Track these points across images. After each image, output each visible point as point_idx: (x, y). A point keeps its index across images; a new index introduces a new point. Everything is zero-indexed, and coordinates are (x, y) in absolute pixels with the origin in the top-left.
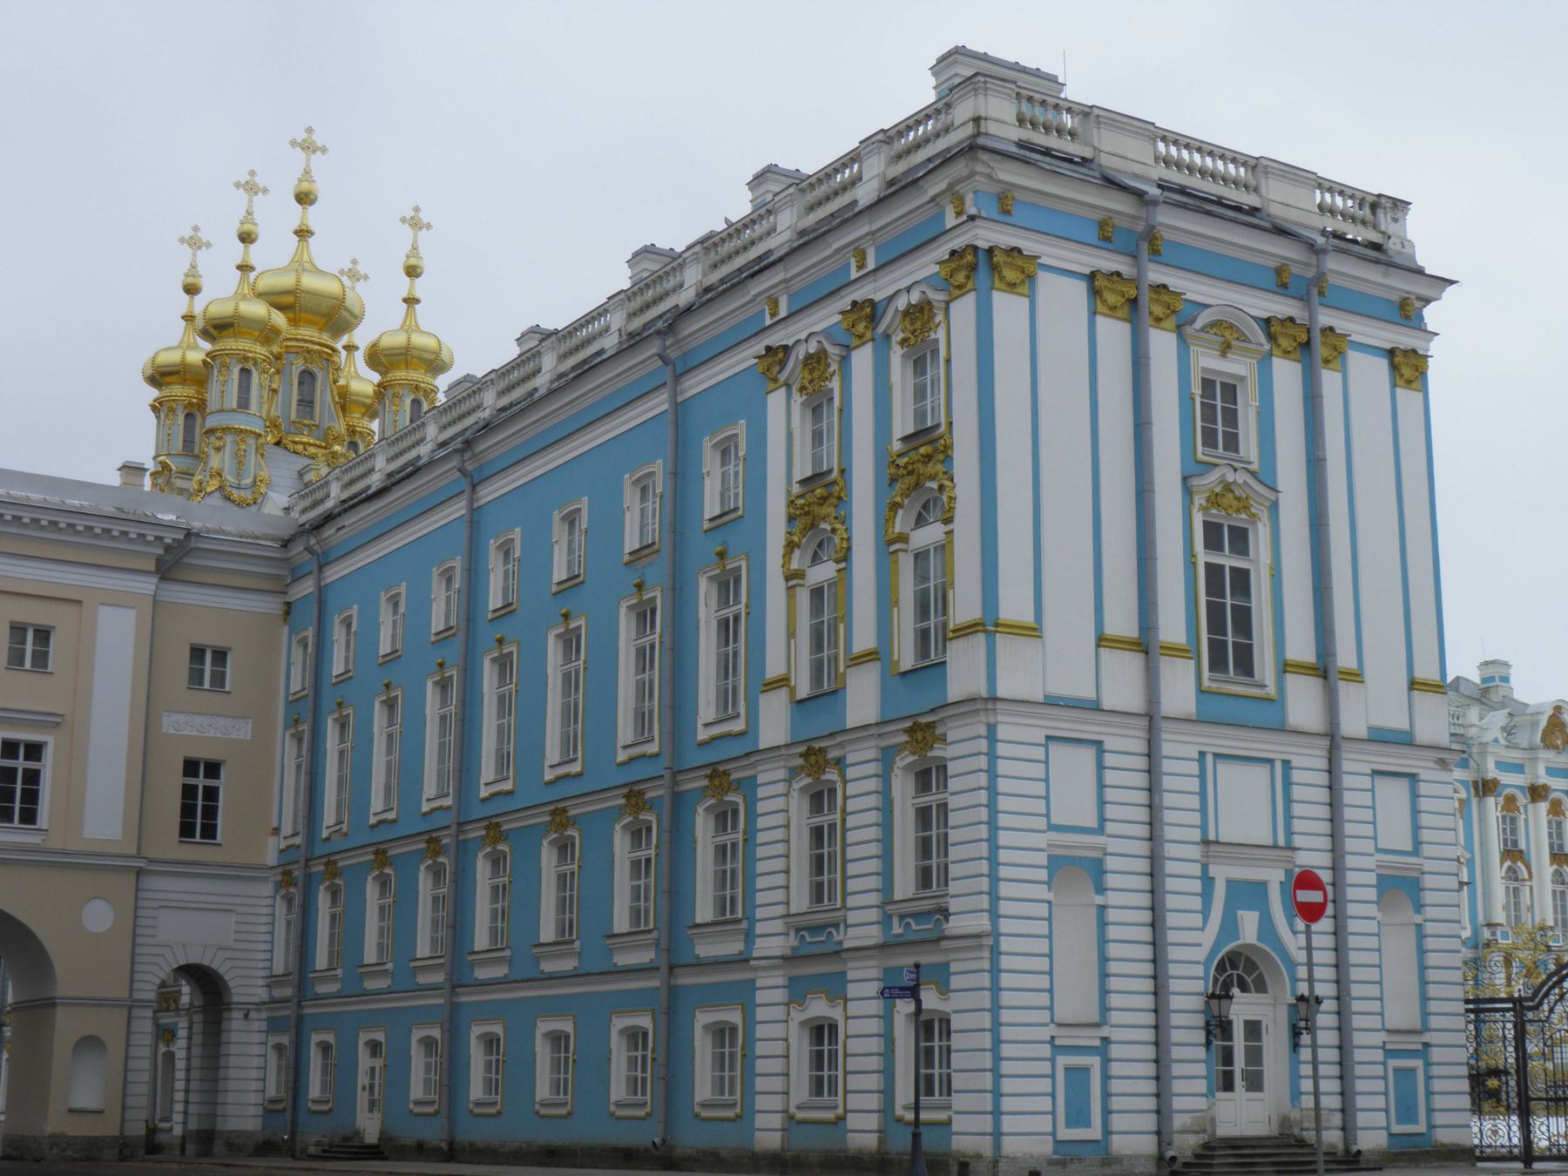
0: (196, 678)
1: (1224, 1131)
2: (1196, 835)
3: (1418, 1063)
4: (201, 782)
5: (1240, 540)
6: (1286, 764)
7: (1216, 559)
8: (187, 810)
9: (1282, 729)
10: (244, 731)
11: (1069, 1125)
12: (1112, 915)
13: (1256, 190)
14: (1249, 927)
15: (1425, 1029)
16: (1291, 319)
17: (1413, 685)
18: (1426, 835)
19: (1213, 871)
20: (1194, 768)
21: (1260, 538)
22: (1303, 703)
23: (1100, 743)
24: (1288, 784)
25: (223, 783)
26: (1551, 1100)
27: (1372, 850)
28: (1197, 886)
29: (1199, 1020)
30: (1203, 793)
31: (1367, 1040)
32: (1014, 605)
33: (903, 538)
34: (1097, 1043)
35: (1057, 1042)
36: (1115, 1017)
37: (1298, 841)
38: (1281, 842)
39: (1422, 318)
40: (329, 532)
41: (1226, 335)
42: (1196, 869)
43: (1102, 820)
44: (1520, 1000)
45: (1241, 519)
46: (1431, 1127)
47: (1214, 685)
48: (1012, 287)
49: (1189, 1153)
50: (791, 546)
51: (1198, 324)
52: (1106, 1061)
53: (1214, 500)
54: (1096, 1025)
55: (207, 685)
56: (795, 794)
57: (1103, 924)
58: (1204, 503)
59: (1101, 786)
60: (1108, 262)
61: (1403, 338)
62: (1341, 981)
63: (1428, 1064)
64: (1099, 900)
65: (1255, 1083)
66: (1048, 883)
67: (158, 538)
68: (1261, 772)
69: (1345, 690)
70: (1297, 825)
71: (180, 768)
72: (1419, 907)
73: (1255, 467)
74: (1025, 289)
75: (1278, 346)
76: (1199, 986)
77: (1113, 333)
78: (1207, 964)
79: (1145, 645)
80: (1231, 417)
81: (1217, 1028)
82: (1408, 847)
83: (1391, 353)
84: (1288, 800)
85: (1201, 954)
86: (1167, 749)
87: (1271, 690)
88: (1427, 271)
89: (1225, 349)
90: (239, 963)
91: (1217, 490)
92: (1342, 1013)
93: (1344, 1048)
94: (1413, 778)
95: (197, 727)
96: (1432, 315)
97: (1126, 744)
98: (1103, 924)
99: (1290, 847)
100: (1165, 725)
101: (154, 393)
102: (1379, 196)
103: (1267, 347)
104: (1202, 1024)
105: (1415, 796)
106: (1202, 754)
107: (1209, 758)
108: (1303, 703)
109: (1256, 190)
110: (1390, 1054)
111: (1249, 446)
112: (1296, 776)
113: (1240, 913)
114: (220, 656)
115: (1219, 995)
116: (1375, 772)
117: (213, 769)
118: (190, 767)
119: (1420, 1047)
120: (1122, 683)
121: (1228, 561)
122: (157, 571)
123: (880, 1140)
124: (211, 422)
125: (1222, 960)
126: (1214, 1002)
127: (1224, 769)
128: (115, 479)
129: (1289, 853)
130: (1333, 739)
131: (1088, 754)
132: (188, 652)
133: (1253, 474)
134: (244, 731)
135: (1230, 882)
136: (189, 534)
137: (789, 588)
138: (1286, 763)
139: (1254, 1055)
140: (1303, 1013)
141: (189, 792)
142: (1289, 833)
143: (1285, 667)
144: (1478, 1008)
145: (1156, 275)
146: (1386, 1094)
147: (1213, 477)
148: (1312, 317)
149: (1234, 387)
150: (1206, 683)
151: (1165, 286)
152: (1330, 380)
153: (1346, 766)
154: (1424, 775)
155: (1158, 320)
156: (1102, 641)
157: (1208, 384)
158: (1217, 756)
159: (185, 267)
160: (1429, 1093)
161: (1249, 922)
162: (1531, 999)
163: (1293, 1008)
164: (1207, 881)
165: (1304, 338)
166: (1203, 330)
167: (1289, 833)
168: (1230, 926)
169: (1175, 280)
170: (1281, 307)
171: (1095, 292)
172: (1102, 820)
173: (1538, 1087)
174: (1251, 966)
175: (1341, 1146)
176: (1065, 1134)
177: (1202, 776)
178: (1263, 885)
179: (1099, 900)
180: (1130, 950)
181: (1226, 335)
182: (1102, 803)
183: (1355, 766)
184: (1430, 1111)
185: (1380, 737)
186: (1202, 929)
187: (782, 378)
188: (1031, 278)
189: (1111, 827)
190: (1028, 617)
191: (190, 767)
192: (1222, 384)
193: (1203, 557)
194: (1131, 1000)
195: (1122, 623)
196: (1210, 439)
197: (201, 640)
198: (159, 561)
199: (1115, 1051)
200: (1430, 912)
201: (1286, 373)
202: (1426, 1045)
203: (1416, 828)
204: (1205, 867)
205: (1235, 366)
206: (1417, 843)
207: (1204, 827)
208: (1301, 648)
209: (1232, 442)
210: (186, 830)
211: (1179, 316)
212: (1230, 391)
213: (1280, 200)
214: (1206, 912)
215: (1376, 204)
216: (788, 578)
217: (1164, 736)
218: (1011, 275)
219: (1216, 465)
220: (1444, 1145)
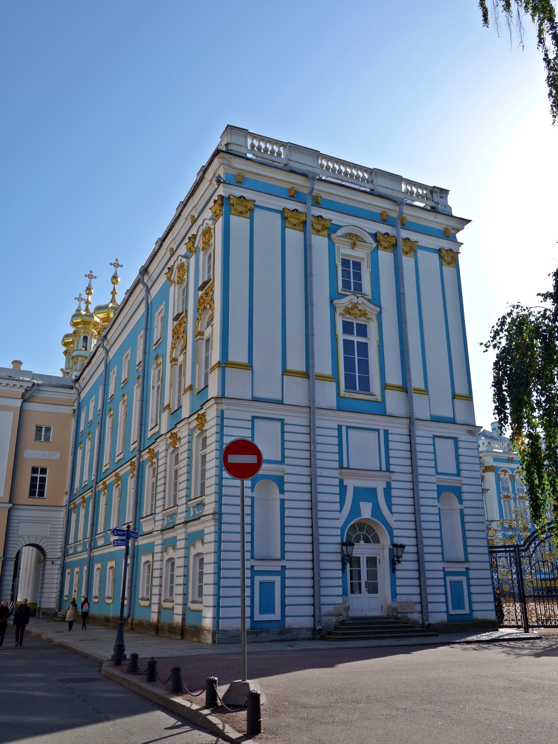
0: (38, 437)
1: (352, 614)
2: (336, 465)
3: (463, 579)
4: (39, 475)
5: (363, 331)
6: (386, 432)
7: (349, 338)
8: (33, 486)
9: (384, 415)
10: (56, 456)
11: (261, 612)
12: (287, 504)
13: (372, 182)
15: (466, 561)
16: (387, 234)
17: (454, 396)
18: (462, 466)
19: (346, 482)
20: (336, 433)
21: (372, 329)
22: (395, 402)
23: (283, 420)
24: (387, 441)
25: (47, 476)
26: (536, 596)
27: (434, 473)
28: (337, 490)
29: (339, 557)
30: (340, 445)
31: (434, 566)
32: (238, 354)
33: (201, 334)
34: (279, 569)
35: (256, 569)
36: (287, 556)
37: (392, 468)
38: (384, 468)
39: (456, 238)
40: (81, 381)
41: (354, 240)
42: (337, 482)
43: (283, 457)
44: (518, 546)
46: (471, 610)
47: (347, 395)
48: (241, 214)
49: (332, 626)
50: (173, 348)
51: (340, 232)
53: (348, 311)
54: (279, 560)
55: (42, 440)
56: (169, 455)
58: (342, 312)
59: (283, 441)
60: (291, 205)
61: (446, 244)
62: (418, 537)
63: (468, 579)
64: (282, 496)
65: (373, 589)
67: (21, 386)
69: (416, 397)
70: (392, 461)
71: (30, 470)
73: (370, 297)
74: (248, 215)
75: (381, 245)
76: (338, 540)
77: (294, 236)
78: (342, 529)
80: (358, 276)
81: (348, 560)
82: (455, 472)
83: (439, 251)
85: (340, 524)
86: (318, 423)
87: (379, 398)
88: (454, 214)
89: (354, 245)
90: (49, 543)
91: (350, 306)
92: (419, 554)
93: (420, 571)
94: (456, 439)
95: (34, 455)
96: (460, 236)
97: (297, 420)
99: (388, 470)
100: (317, 411)
101: (65, 349)
102: (434, 187)
103: (375, 245)
104: (340, 559)
105: (457, 448)
106: (340, 427)
107: (344, 429)
108: (395, 402)
109: (372, 182)
110: (447, 574)
111: (367, 287)
112: (391, 437)
113: (361, 503)
114: (48, 430)
115: (348, 544)
116: (434, 437)
117: (44, 471)
118: (35, 470)
119: (464, 570)
120: (296, 391)
121: (356, 339)
122: (22, 398)
123: (184, 619)
124: (74, 354)
125: (353, 526)
126: (344, 548)
127: (351, 432)
128: (11, 366)
129: (388, 474)
130: (411, 420)
132: (35, 428)
133: (369, 300)
134: (56, 456)
135: (356, 489)
136: (34, 384)
137: (172, 366)
138: (386, 432)
139: (373, 575)
140: (396, 553)
141: (34, 479)
143: (385, 387)
144: (492, 550)
145: (316, 211)
146: (446, 594)
147: (347, 299)
148: (398, 232)
149: (360, 263)
150: (342, 393)
151: (321, 217)
152: (407, 262)
153: (418, 433)
154: (461, 438)
155: (318, 231)
156: (285, 372)
157: (345, 262)
158: (348, 427)
159: (77, 307)
160: (470, 594)
162: (523, 546)
163: (391, 551)
164: (343, 488)
165: (394, 241)
166: (341, 236)
167: (388, 464)
168: (355, 510)
169: (326, 214)
170: (383, 229)
171: (284, 218)
173: (528, 589)
174: (371, 530)
175: (421, 622)
178: (374, 490)
179: (282, 496)
180: (299, 520)
181: (354, 240)
182: (283, 449)
183: (423, 432)
184: (471, 603)
185: (436, 419)
186: (340, 511)
187: (172, 279)
188: (251, 210)
189: (287, 461)
190: (244, 360)
191: (35, 470)
192: (353, 261)
193: (341, 337)
194: (298, 548)
195: (296, 362)
196: (346, 285)
197: (40, 423)
198: (23, 395)
199: (288, 573)
200: (466, 503)
201: (385, 258)
202: (467, 569)
203: (458, 463)
204: (341, 481)
205: (360, 254)
206: (459, 471)
207: (341, 461)
208: (394, 377)
209: (358, 287)
210: (32, 494)
211: (330, 229)
212: (357, 265)
213: (382, 185)
214: (342, 503)
215: (433, 190)
216: (171, 362)
217: (317, 417)
218: (241, 209)
219: (347, 295)
220: (480, 620)
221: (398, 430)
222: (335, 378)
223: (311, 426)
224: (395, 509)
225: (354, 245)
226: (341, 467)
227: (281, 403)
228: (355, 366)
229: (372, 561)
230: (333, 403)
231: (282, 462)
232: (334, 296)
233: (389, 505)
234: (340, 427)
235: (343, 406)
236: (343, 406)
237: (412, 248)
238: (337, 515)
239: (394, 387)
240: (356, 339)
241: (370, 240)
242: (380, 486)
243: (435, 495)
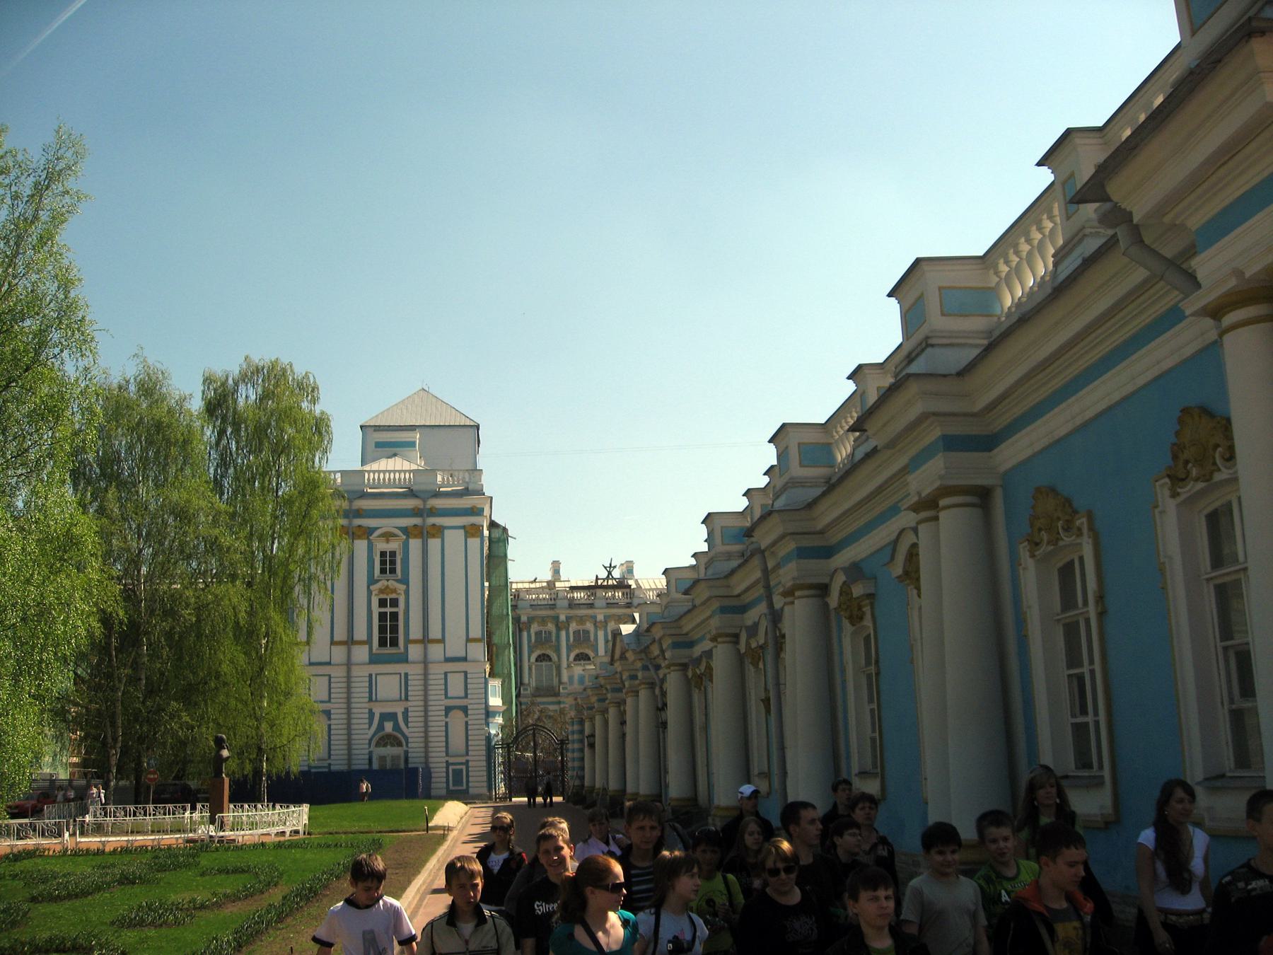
5: (395, 603)
22: (415, 652)
41: (388, 536)
45: (394, 596)
51: (376, 534)
53: (381, 591)
72: (467, 715)
79: (350, 642)
82: (462, 694)
85: (369, 736)
106: (370, 676)
120: (339, 654)
121: (388, 610)
138: (406, 675)
156: (333, 643)
161: (389, 727)
168: (381, 727)
181: (388, 536)
183: (437, 670)
195: (340, 634)
196: (383, 571)
204: (370, 711)
205: (393, 546)
208: (416, 632)
209: (393, 571)
211: (367, 533)
212: (393, 554)
214: (370, 724)
221: (414, 671)
222: (369, 642)
223: (349, 677)
225: (388, 541)
226: (371, 700)
227: (329, 663)
228: (389, 630)
230: (366, 659)
231: (329, 701)
232: (371, 581)
233: (406, 722)
234: (370, 676)
235: (374, 659)
236: (374, 659)
237: (439, 531)
239: (416, 642)
241: (400, 533)
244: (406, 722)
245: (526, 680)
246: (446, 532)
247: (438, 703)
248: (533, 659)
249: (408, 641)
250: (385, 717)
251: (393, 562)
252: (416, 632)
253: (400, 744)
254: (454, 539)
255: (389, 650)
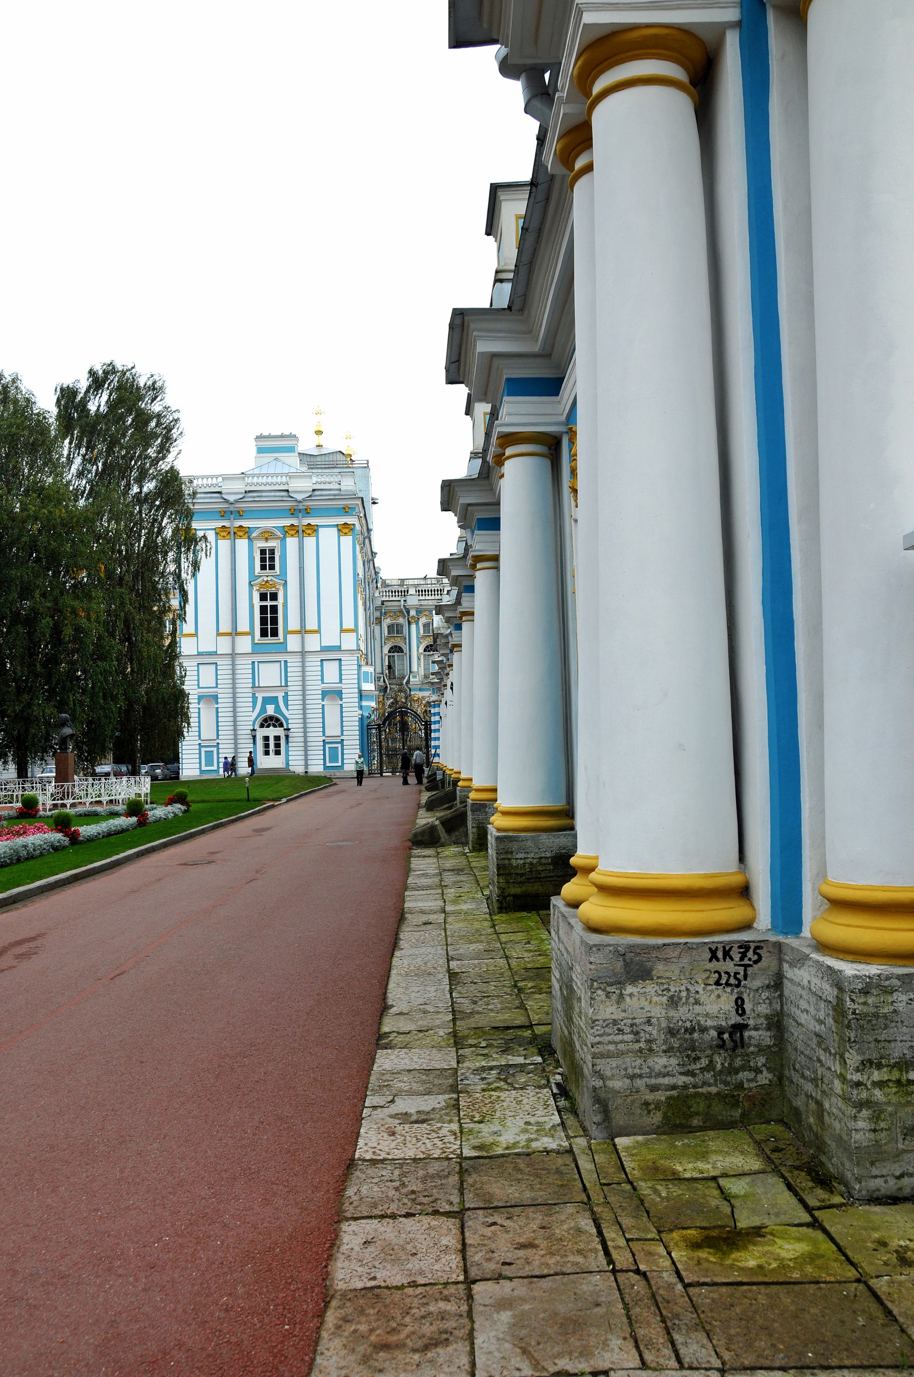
2: (251, 685)
5: (274, 597)
6: (286, 661)
12: (220, 710)
14: (270, 710)
20: (250, 666)
22: (293, 643)
24: (286, 667)
42: (251, 695)
43: (217, 684)
52: (218, 749)
53: (261, 586)
57: (217, 712)
66: (199, 703)
68: (278, 664)
72: (341, 699)
84: (286, 672)
85: (253, 718)
87: (282, 640)
98: (217, 712)
105: (340, 665)
106: (253, 662)
120: (224, 645)
121: (269, 603)
131: (214, 666)
138: (286, 661)
139: (278, 745)
142: (286, 681)
147: (261, 579)
167: (286, 681)
172: (217, 684)
176: (204, 768)
177: (253, 669)
195: (225, 627)
196: (263, 567)
199: (220, 746)
202: (342, 740)
204: (254, 694)
207: (254, 683)
208: (294, 624)
214: (254, 707)
222: (251, 633)
224: (290, 707)
228: (269, 622)
229: (277, 738)
230: (249, 649)
231: (217, 687)
233: (287, 705)
234: (253, 662)
235: (257, 649)
238: (250, 714)
240: (269, 603)
242: (280, 695)
243: (320, 697)
244: (287, 705)
245: (415, 669)
246: (320, 529)
247: (315, 688)
248: (421, 650)
249: (287, 632)
250: (266, 701)
251: (272, 559)
252: (294, 624)
253: (281, 725)
254: (328, 536)
255: (269, 640)
